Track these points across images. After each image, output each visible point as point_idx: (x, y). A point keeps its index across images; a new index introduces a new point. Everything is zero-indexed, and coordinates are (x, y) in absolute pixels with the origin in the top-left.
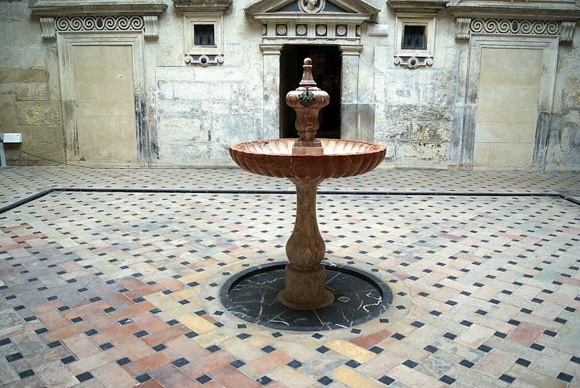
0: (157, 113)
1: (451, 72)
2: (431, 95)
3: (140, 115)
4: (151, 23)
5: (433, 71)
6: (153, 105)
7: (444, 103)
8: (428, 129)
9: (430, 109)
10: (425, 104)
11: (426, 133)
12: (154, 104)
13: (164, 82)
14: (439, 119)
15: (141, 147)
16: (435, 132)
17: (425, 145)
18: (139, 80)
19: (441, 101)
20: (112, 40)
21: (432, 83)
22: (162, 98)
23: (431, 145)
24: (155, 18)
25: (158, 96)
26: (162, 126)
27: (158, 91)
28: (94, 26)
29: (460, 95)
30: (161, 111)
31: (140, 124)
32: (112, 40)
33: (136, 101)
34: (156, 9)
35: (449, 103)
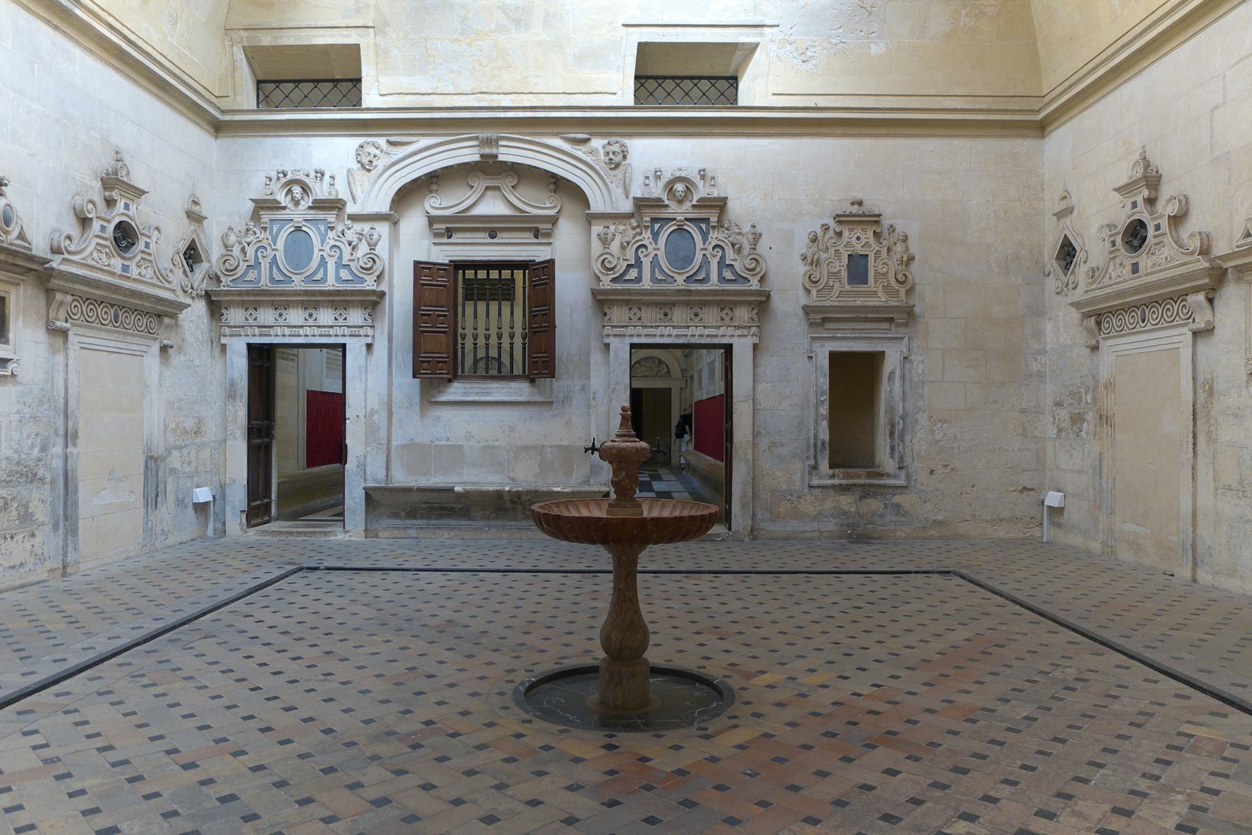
1: (42, 389)
2: (16, 436)
5: (19, 388)
7: (36, 450)
8: (16, 505)
9: (18, 463)
10: (9, 453)
11: (14, 513)
14: (32, 482)
16: (26, 507)
17: (12, 538)
19: (32, 446)
21: (18, 412)
23: (21, 536)
29: (56, 433)
35: (44, 449)
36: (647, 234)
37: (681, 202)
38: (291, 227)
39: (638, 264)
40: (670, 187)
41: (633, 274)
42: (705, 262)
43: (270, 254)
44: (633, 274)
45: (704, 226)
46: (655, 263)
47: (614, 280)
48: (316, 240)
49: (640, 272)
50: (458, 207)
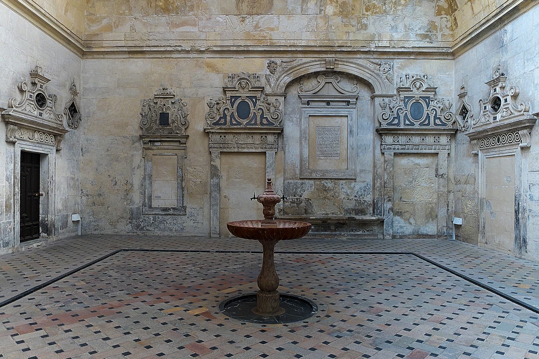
0: (528, 211)
3: (517, 212)
4: (524, 135)
6: (525, 204)
12: (525, 203)
13: (533, 185)
15: (516, 240)
18: (517, 182)
20: (505, 152)
22: (531, 198)
24: (525, 131)
25: (529, 197)
26: (530, 223)
27: (529, 193)
28: (496, 143)
30: (530, 211)
31: (516, 220)
32: (505, 152)
33: (516, 200)
34: (525, 123)
36: (402, 103)
37: (418, 89)
38: (240, 99)
39: (398, 117)
40: (414, 83)
41: (396, 121)
42: (428, 117)
43: (231, 111)
44: (396, 121)
45: (427, 100)
46: (406, 116)
47: (388, 124)
48: (251, 104)
49: (399, 120)
50: (313, 91)
